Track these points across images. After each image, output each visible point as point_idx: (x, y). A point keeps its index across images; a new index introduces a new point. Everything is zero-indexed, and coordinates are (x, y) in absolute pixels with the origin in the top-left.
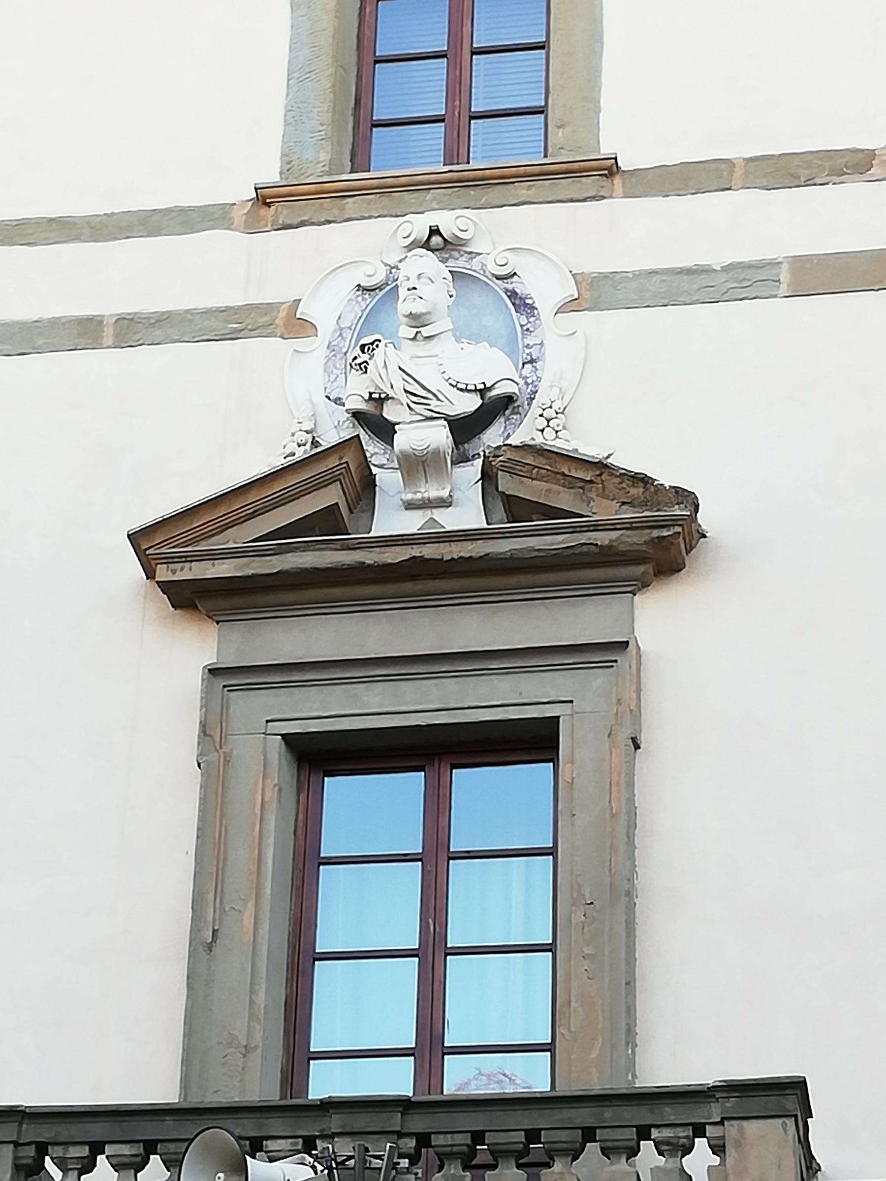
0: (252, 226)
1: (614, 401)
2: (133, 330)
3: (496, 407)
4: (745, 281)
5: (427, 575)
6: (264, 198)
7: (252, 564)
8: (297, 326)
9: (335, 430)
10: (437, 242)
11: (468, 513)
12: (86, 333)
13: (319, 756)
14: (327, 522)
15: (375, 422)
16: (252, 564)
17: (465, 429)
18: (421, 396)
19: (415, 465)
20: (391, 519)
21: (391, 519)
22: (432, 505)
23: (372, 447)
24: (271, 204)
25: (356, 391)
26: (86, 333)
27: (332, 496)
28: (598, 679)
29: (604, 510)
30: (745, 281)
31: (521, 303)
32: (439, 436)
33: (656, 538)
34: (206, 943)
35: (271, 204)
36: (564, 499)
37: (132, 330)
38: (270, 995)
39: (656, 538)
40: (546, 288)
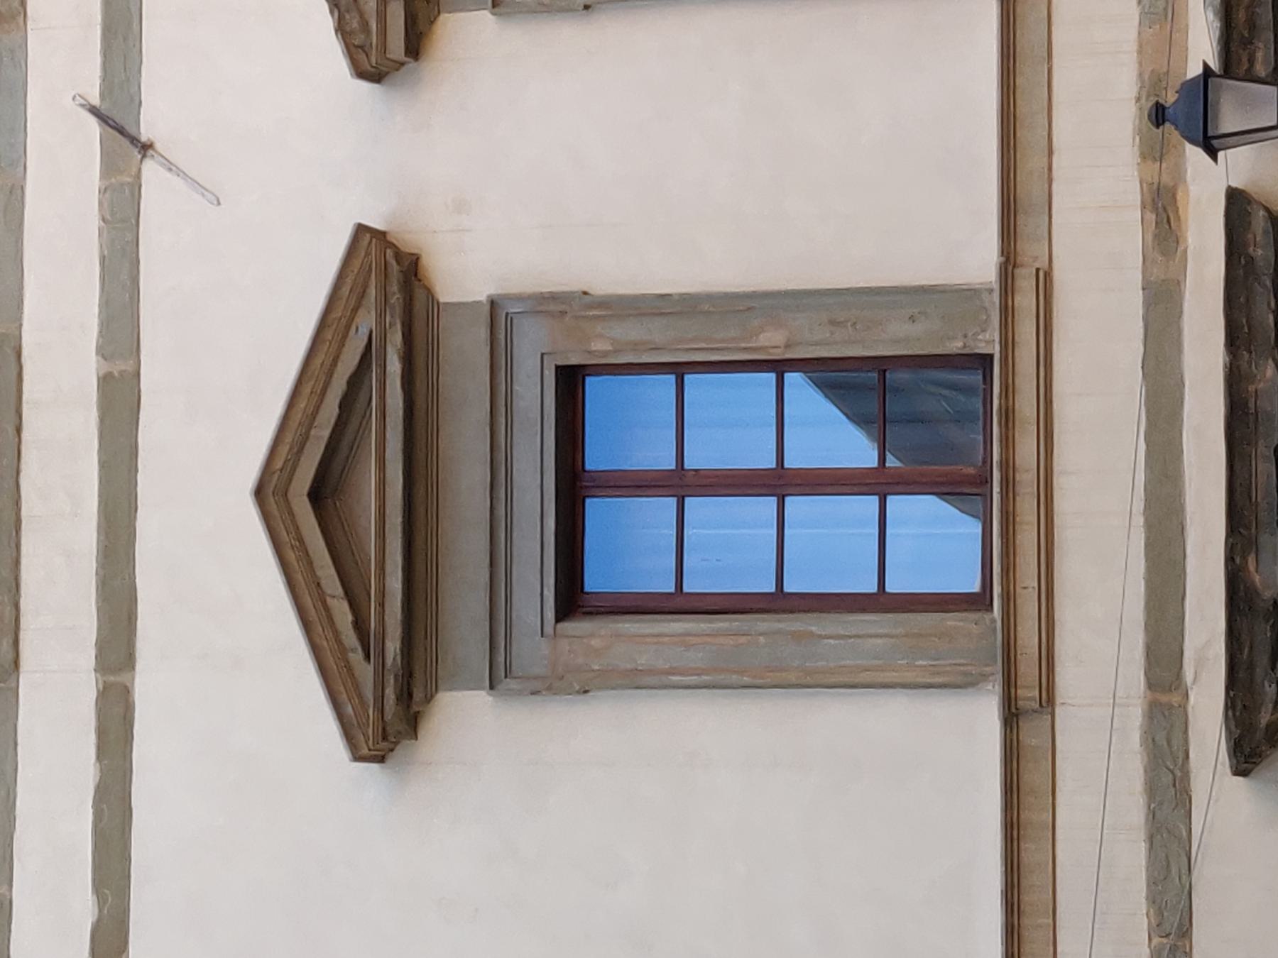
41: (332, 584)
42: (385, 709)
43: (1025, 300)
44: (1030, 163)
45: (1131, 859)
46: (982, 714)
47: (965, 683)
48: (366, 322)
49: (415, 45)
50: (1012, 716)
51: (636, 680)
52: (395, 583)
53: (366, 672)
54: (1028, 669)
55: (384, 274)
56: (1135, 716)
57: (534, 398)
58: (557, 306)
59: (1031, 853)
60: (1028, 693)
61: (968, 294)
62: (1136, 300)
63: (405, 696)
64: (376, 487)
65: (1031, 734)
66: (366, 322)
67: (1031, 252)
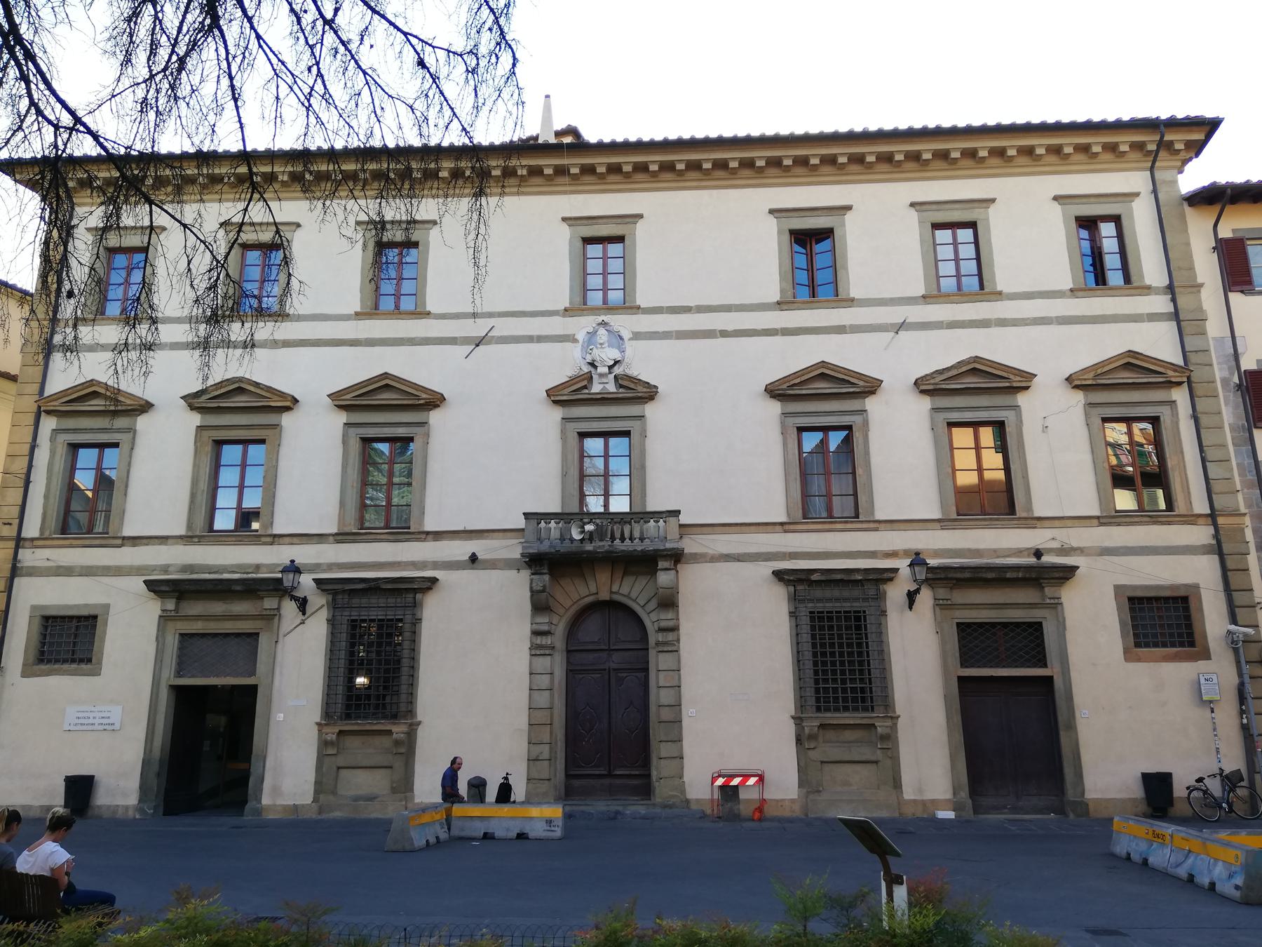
0: (564, 316)
1: (644, 363)
2: (540, 339)
3: (616, 362)
4: (666, 335)
5: (603, 400)
6: (566, 310)
7: (570, 396)
8: (575, 341)
9: (586, 369)
10: (603, 324)
11: (611, 387)
12: (530, 339)
13: (583, 435)
14: (585, 387)
15: (592, 364)
16: (570, 396)
17: (610, 367)
18: (603, 361)
19: (601, 375)
20: (596, 388)
21: (596, 388)
22: (603, 385)
23: (593, 370)
24: (567, 312)
25: (589, 359)
26: (530, 339)
27: (585, 383)
28: (638, 423)
29: (640, 388)
30: (666, 335)
31: (621, 338)
32: (606, 370)
33: (648, 394)
34: (564, 475)
35: (567, 312)
36: (632, 386)
37: (540, 339)
38: (576, 485)
39: (648, 394)
40: (626, 335)
41: (803, 378)
42: (775, 392)
43: (872, 525)
44: (902, 526)
45: (753, 549)
46: (783, 518)
47: (788, 515)
48: (861, 383)
49: (923, 392)
50: (782, 524)
51: (785, 444)
52: (804, 392)
53: (785, 386)
54: (792, 527)
55: (871, 387)
56: (784, 550)
57: (845, 420)
58: (866, 424)
59: (753, 528)
60: (787, 527)
61: (873, 513)
62: (872, 549)
63: (780, 395)
64: (823, 387)
65: (778, 528)
66: (861, 383)
67: (882, 526)
